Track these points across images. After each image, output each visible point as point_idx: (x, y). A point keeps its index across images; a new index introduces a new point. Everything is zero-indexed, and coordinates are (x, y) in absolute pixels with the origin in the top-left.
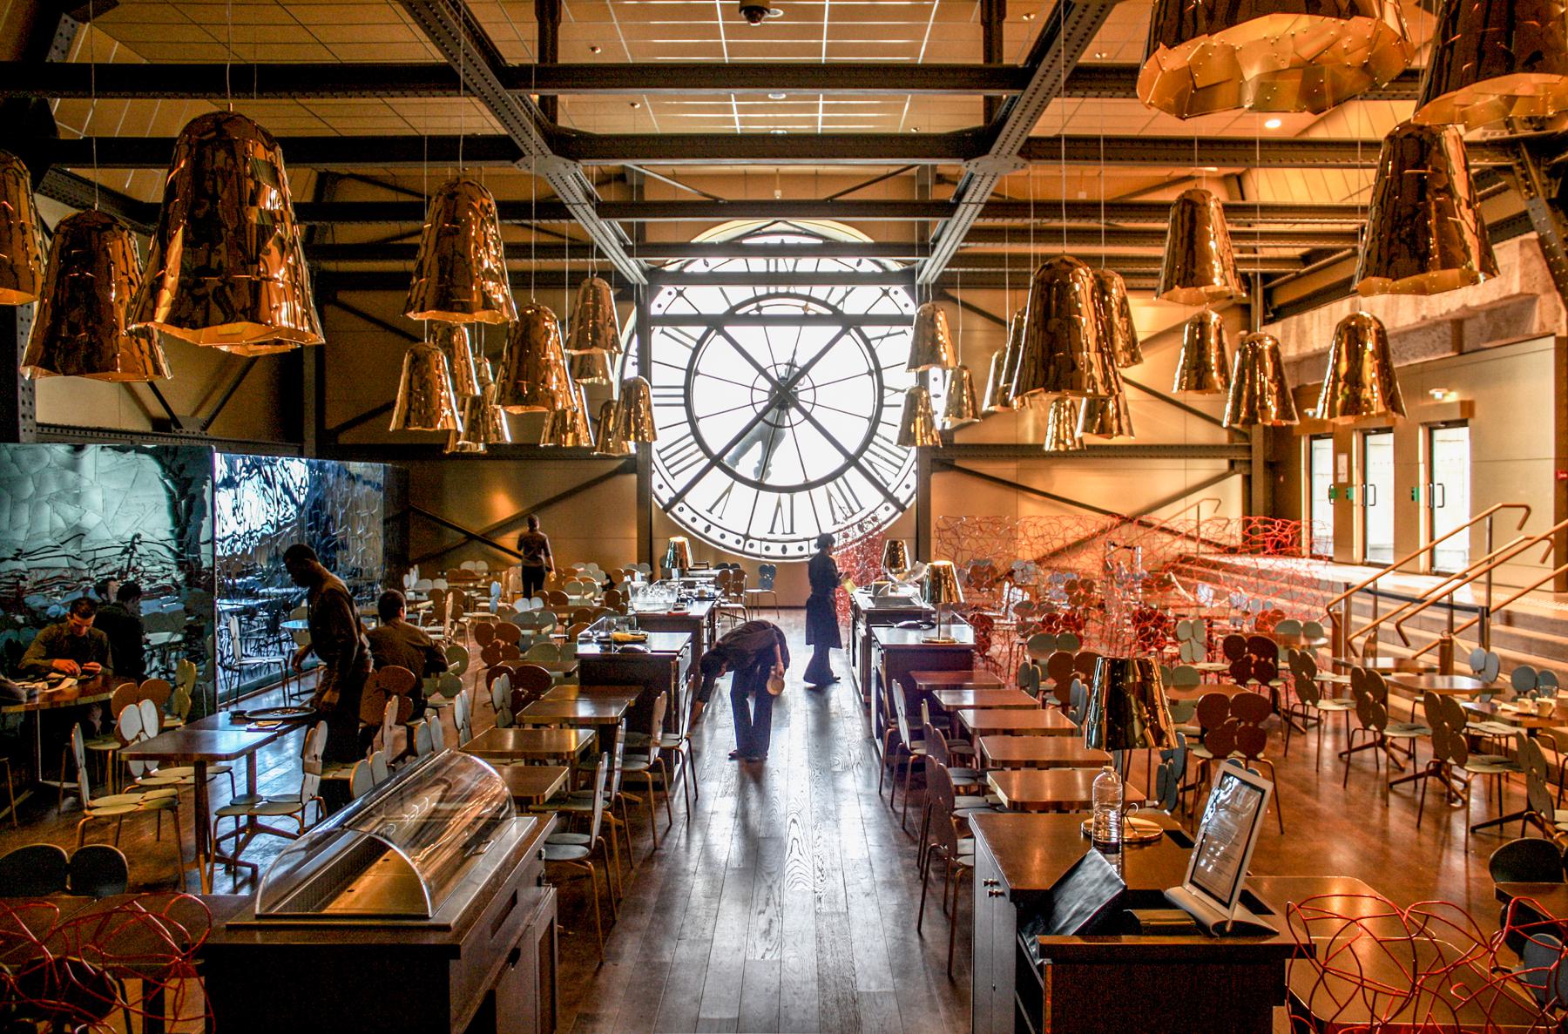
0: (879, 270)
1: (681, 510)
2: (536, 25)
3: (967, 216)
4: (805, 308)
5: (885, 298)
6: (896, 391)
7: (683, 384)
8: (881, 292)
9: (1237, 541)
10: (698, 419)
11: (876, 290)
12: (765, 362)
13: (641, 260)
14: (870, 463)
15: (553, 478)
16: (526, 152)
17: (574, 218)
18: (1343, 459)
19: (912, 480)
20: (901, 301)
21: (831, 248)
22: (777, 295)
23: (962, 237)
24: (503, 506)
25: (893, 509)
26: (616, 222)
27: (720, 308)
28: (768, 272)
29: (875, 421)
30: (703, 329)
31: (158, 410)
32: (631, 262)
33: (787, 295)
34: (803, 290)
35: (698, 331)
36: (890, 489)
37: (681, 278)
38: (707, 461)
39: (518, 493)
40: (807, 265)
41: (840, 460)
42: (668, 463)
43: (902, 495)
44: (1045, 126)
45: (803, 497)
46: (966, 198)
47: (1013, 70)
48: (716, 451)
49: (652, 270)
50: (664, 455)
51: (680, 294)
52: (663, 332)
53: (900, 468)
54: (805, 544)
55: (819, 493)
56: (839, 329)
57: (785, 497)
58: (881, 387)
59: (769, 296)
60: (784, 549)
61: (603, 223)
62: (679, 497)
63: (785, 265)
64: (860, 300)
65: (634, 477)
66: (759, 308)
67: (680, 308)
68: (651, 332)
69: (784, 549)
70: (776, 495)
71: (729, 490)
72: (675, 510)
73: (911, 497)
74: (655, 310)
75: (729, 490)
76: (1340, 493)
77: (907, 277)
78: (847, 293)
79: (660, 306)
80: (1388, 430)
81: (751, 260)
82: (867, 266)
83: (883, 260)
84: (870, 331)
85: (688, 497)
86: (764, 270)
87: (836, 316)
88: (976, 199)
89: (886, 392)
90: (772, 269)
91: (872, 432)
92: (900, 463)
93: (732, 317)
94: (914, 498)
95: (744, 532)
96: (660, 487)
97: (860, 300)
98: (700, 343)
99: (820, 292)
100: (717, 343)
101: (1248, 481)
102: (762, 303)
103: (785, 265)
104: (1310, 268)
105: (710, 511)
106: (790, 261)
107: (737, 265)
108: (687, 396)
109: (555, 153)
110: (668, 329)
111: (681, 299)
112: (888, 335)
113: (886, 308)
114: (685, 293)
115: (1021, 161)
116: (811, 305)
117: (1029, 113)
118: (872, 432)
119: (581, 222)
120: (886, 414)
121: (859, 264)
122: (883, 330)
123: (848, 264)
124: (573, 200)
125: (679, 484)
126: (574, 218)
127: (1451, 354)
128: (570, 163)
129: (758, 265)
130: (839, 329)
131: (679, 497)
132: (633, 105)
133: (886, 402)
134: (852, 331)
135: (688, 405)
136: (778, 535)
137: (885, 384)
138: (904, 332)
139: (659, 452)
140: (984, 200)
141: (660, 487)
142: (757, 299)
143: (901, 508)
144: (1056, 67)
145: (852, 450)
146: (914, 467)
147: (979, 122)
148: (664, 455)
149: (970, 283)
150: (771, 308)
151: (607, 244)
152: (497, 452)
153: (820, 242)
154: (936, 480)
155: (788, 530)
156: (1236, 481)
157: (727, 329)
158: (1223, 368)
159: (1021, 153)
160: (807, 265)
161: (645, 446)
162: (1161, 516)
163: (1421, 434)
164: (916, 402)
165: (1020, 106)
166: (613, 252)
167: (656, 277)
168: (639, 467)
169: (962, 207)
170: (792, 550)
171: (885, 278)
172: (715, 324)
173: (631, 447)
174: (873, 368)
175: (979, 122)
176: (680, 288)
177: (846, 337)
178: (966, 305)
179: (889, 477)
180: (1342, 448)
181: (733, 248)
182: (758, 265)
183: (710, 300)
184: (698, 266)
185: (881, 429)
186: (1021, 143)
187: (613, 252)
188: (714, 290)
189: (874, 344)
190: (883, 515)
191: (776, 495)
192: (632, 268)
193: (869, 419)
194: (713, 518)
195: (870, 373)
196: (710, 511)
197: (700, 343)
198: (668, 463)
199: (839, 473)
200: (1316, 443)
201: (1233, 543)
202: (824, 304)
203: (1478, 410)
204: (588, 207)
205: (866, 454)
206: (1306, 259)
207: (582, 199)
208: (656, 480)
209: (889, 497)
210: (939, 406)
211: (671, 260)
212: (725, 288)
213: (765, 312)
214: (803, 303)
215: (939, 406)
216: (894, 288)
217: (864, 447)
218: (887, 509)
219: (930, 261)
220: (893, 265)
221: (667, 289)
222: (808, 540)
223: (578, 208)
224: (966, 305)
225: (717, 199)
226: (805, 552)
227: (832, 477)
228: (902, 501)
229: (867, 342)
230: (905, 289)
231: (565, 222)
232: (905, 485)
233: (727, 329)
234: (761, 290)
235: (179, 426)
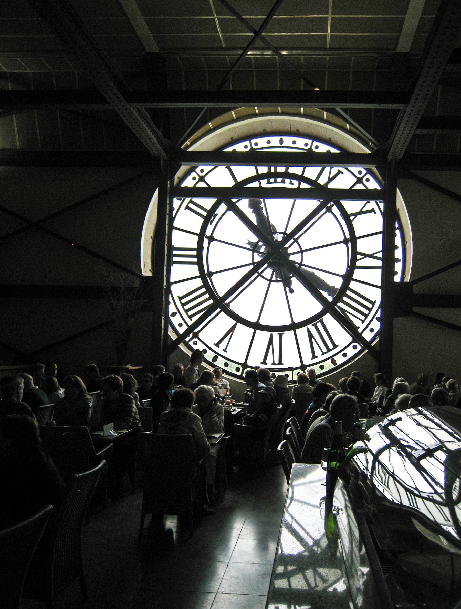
1: (195, 343)
6: (365, 256)
7: (195, 246)
19: (376, 325)
30: (213, 201)
42: (187, 307)
43: (368, 336)
45: (288, 335)
50: (184, 301)
53: (366, 316)
55: (302, 332)
57: (276, 335)
70: (268, 334)
89: (359, 257)
95: (242, 361)
98: (211, 213)
105: (217, 345)
108: (199, 256)
135: (200, 263)
146: (379, 315)
155: (277, 361)
174: (348, 236)
179: (357, 323)
190: (351, 352)
191: (269, 333)
194: (220, 351)
195: (345, 241)
196: (217, 345)
197: (211, 213)
198: (187, 307)
199: (318, 317)
212: (232, 168)
218: (355, 347)
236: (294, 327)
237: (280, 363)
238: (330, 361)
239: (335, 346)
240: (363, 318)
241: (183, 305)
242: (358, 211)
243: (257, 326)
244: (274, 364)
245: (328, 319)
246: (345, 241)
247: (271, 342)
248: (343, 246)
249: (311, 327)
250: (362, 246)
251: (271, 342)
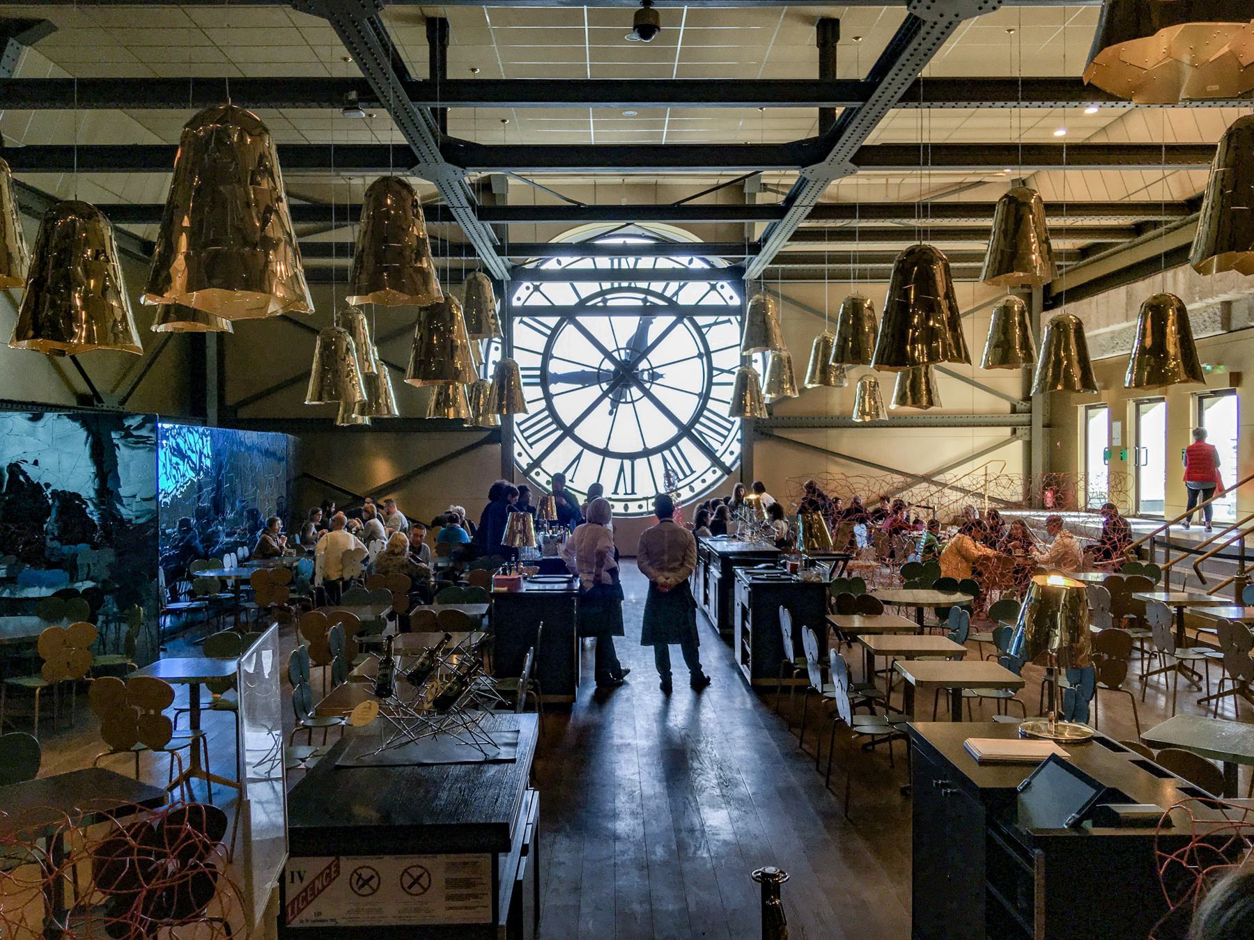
0: (707, 267)
1: (538, 474)
2: (427, 48)
3: (797, 218)
4: (645, 300)
5: (713, 293)
6: (722, 371)
8: (708, 287)
9: (1018, 498)
10: (553, 396)
11: (704, 286)
12: (610, 347)
13: (505, 258)
14: (700, 433)
15: (427, 447)
16: (421, 159)
17: (455, 220)
18: (1117, 426)
19: (737, 448)
20: (727, 293)
21: (664, 247)
22: (620, 289)
23: (788, 237)
24: (382, 471)
25: (719, 473)
26: (488, 224)
27: (572, 301)
28: (612, 270)
29: (705, 397)
30: (558, 318)
31: (83, 388)
32: (498, 259)
33: (629, 289)
34: (643, 285)
35: (552, 321)
36: (718, 454)
37: (539, 276)
38: (560, 432)
39: (397, 458)
40: (646, 263)
41: (673, 431)
42: (526, 434)
43: (728, 460)
44: (875, 137)
45: (641, 463)
46: (797, 203)
47: (856, 82)
48: (568, 422)
49: (514, 267)
50: (522, 427)
51: (537, 289)
52: (521, 322)
53: (725, 437)
54: (644, 503)
55: (656, 460)
56: (674, 318)
57: (627, 463)
58: (711, 368)
59: (613, 290)
60: (626, 507)
61: (478, 224)
62: (536, 463)
63: (628, 263)
64: (691, 294)
65: (498, 447)
66: (605, 301)
67: (537, 300)
68: (513, 320)
69: (626, 507)
71: (578, 457)
72: (533, 474)
73: (735, 462)
74: (515, 303)
75: (578, 457)
76: (1115, 455)
77: (735, 274)
78: (681, 288)
79: (519, 299)
80: (1162, 400)
81: (597, 259)
82: (698, 264)
83: (710, 258)
84: (701, 320)
85: (544, 464)
86: (609, 267)
87: (672, 307)
88: (805, 203)
89: (715, 373)
90: (616, 266)
91: (703, 408)
92: (725, 433)
93: (583, 307)
94: (739, 463)
96: (520, 454)
97: (691, 294)
98: (555, 332)
99: (657, 286)
100: (569, 330)
101: (1028, 446)
102: (608, 297)
103: (628, 263)
104: (1085, 261)
106: (632, 260)
107: (586, 263)
109: (446, 161)
110: (526, 319)
111: (537, 294)
112: (716, 323)
113: (713, 300)
114: (542, 288)
115: (852, 166)
116: (650, 298)
117: (865, 123)
118: (703, 408)
119: (461, 224)
120: (715, 392)
121: (690, 262)
122: (711, 319)
123: (683, 261)
124: (457, 204)
125: (536, 451)
126: (455, 220)
127: (1221, 332)
128: (459, 170)
129: (603, 263)
130: (671, 319)
131: (536, 463)
132: (504, 121)
133: (715, 380)
134: (686, 321)
136: (621, 496)
137: (715, 365)
138: (729, 321)
139: (519, 425)
140: (813, 204)
141: (520, 454)
142: (603, 293)
143: (727, 470)
144: (896, 81)
145: (685, 420)
146: (739, 436)
147: (816, 134)
148: (522, 427)
149: (789, 276)
150: (615, 301)
151: (481, 244)
152: (382, 426)
153: (653, 242)
154: (759, 449)
155: (629, 491)
156: (1017, 447)
157: (579, 319)
158: (1025, 345)
159: (852, 161)
160: (646, 263)
161: (508, 420)
162: (948, 477)
163: (1192, 404)
164: (745, 382)
165: (860, 116)
166: (485, 251)
167: (517, 274)
168: (502, 436)
169: (793, 209)
170: (633, 508)
171: (712, 274)
172: (567, 314)
173: (497, 420)
174: (702, 351)
175: (816, 134)
176: (537, 283)
177: (680, 326)
178: (785, 298)
179: (715, 445)
180: (1117, 415)
181: (586, 248)
182: (603, 263)
183: (561, 293)
184: (551, 264)
185: (711, 404)
186: (855, 150)
187: (485, 251)
188: (566, 286)
189: (704, 330)
190: (710, 478)
192: (498, 265)
193: (700, 395)
195: (700, 356)
198: (526, 434)
199: (674, 442)
200: (1091, 412)
201: (1015, 499)
202: (660, 296)
203: (1246, 380)
204: (469, 210)
205: (698, 426)
206: (1084, 252)
207: (465, 203)
208: (517, 448)
209: (716, 461)
210: (764, 383)
211: (531, 259)
213: (609, 303)
214: (642, 296)
215: (764, 383)
216: (721, 283)
217: (695, 419)
219: (757, 258)
220: (721, 262)
221: (526, 284)
222: (646, 499)
223: (460, 211)
224: (785, 298)
225: (579, 204)
226: (644, 509)
227: (667, 446)
228: (728, 464)
229: (698, 329)
230: (732, 284)
231: (446, 223)
232: (730, 450)
233: (579, 319)
234: (606, 285)
235: (100, 401)
236: (647, 453)
237: (633, 493)
238: (688, 487)
239: (693, 472)
240: (722, 439)
241: (522, 432)
242: (713, 328)
243: (605, 453)
244: (626, 494)
245: (685, 443)
246: (700, 356)
247: (622, 469)
248: (698, 360)
249: (667, 453)
250: (717, 360)
251: (622, 469)
